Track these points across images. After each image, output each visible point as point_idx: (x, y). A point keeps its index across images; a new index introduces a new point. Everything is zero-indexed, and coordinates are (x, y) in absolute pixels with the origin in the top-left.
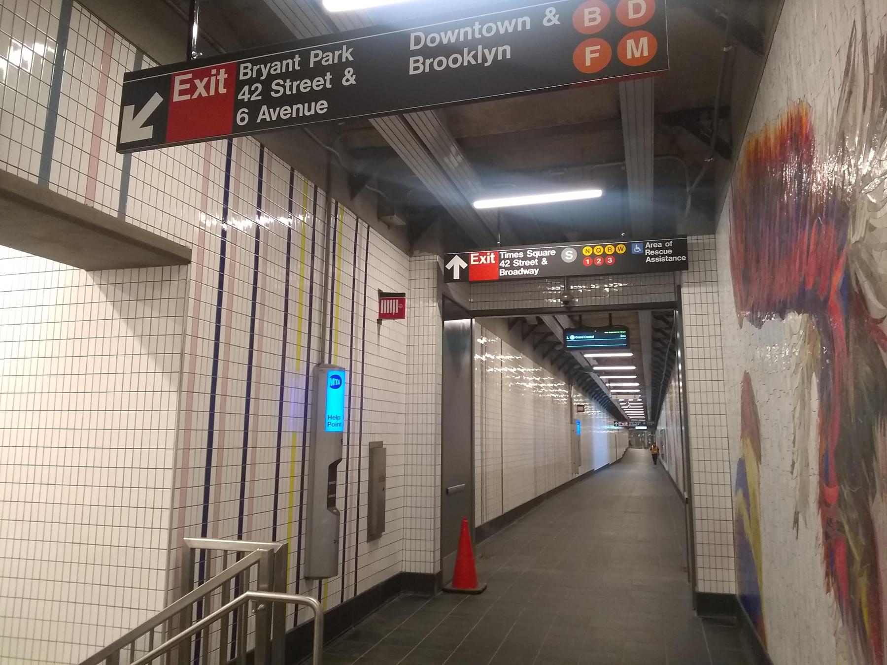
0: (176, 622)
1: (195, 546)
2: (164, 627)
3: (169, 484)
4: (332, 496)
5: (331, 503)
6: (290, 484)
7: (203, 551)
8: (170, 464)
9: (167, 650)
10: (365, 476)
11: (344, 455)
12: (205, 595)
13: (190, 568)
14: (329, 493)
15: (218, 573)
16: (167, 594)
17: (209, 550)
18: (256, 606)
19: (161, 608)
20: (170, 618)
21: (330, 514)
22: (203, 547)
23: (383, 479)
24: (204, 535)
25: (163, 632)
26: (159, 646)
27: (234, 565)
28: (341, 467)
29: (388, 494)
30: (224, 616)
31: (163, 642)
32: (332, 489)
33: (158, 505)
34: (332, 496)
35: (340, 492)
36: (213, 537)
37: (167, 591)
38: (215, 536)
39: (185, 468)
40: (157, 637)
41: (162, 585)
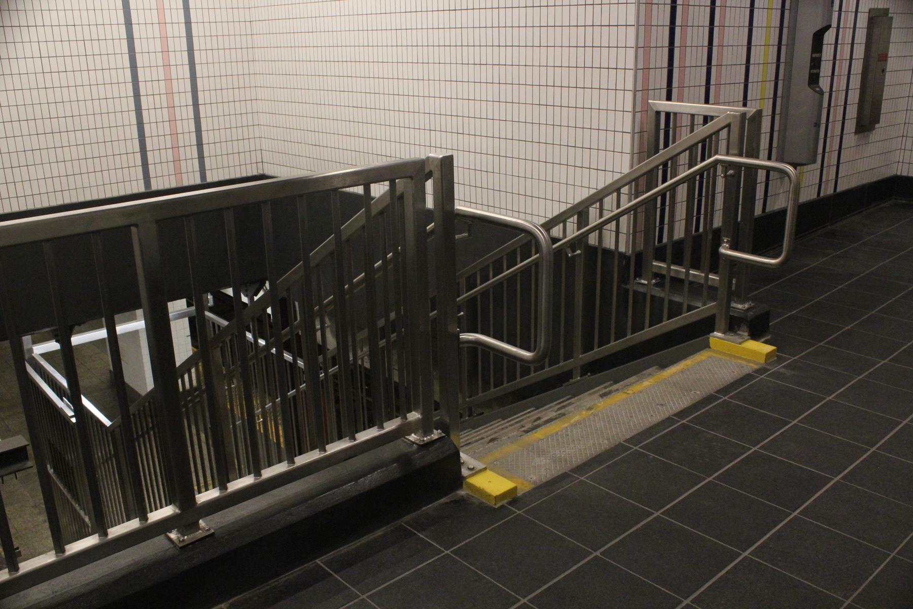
0: (643, 182)
1: (660, 109)
2: (630, 189)
3: (631, 42)
4: (815, 71)
5: (814, 79)
6: (764, 54)
7: (668, 115)
8: (632, 20)
9: (634, 208)
10: (859, 52)
11: (834, 24)
12: (671, 158)
13: (656, 132)
14: (811, 68)
15: (685, 138)
16: (632, 159)
17: (675, 114)
18: (725, 170)
19: (626, 170)
20: (636, 180)
21: (809, 91)
22: (668, 110)
23: (884, 58)
24: (669, 98)
25: (630, 194)
26: (625, 205)
27: (702, 131)
28: (829, 37)
29: (889, 78)
30: (689, 179)
31: (630, 201)
32: (816, 63)
33: (621, 65)
34: (815, 71)
35: (825, 69)
36: (678, 101)
37: (633, 154)
38: (680, 99)
39: (648, 26)
40: (624, 198)
41: (627, 148)
